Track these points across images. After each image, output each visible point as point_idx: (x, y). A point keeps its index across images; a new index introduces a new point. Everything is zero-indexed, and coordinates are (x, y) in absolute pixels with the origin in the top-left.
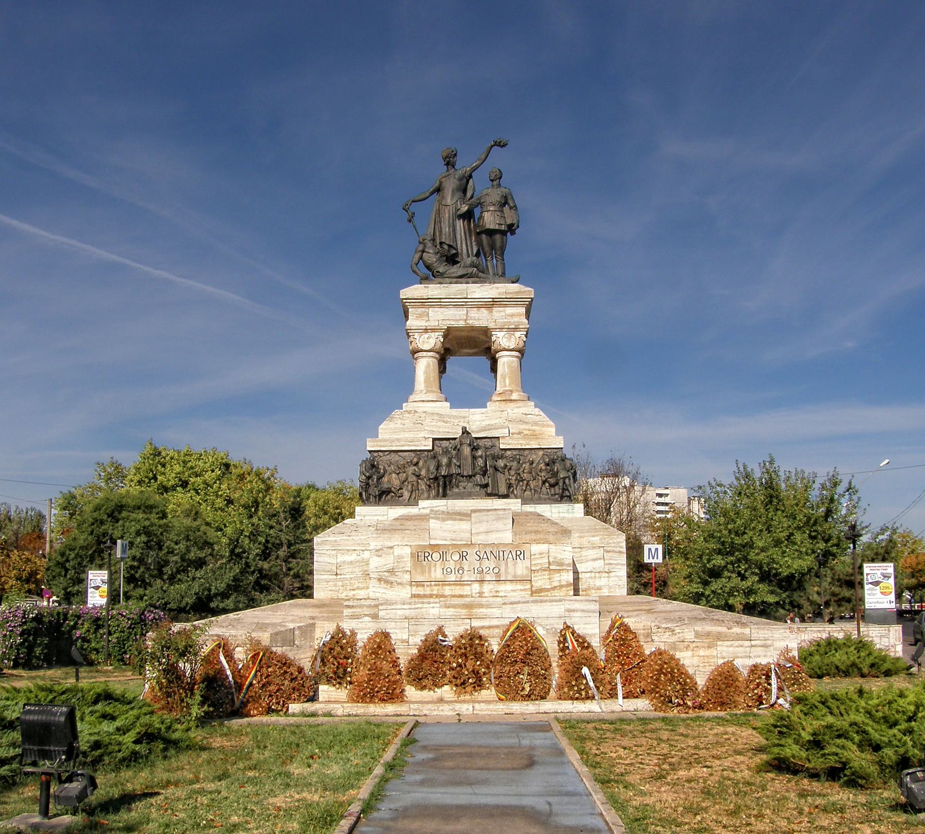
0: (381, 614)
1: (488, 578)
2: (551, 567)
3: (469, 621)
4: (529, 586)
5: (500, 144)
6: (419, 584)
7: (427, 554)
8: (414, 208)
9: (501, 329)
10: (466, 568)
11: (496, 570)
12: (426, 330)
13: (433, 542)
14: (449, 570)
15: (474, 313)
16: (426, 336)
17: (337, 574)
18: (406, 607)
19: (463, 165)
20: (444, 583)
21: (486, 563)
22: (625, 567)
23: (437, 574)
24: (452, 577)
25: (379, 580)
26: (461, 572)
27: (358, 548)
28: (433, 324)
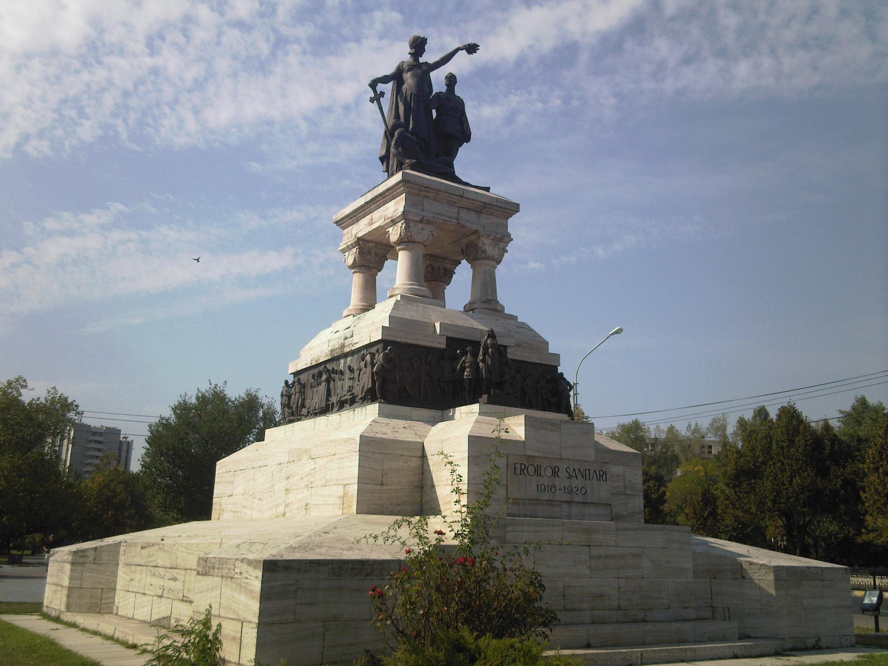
0: (509, 536)
1: (577, 498)
2: (628, 492)
3: (587, 549)
4: (608, 512)
5: (472, 49)
6: (516, 502)
7: (523, 467)
8: (380, 87)
9: (488, 236)
10: (558, 488)
11: (583, 491)
12: (421, 221)
13: (528, 453)
14: (543, 487)
15: (464, 214)
16: (420, 226)
17: (382, 484)
18: (532, 528)
19: (429, 57)
20: (537, 501)
21: (577, 483)
22: (642, 499)
23: (532, 492)
24: (546, 496)
25: (476, 494)
26: (553, 490)
27: (406, 453)
28: (429, 215)
